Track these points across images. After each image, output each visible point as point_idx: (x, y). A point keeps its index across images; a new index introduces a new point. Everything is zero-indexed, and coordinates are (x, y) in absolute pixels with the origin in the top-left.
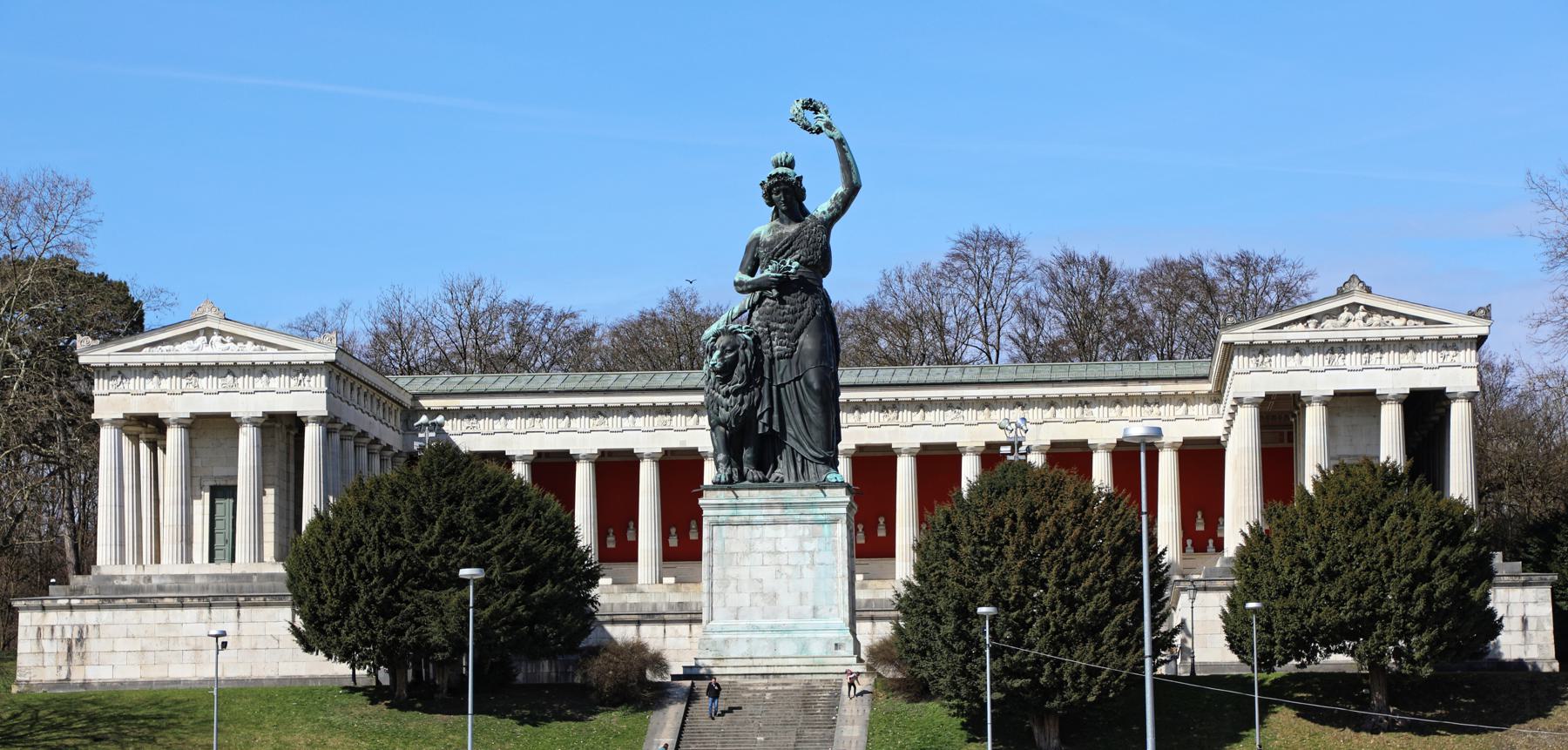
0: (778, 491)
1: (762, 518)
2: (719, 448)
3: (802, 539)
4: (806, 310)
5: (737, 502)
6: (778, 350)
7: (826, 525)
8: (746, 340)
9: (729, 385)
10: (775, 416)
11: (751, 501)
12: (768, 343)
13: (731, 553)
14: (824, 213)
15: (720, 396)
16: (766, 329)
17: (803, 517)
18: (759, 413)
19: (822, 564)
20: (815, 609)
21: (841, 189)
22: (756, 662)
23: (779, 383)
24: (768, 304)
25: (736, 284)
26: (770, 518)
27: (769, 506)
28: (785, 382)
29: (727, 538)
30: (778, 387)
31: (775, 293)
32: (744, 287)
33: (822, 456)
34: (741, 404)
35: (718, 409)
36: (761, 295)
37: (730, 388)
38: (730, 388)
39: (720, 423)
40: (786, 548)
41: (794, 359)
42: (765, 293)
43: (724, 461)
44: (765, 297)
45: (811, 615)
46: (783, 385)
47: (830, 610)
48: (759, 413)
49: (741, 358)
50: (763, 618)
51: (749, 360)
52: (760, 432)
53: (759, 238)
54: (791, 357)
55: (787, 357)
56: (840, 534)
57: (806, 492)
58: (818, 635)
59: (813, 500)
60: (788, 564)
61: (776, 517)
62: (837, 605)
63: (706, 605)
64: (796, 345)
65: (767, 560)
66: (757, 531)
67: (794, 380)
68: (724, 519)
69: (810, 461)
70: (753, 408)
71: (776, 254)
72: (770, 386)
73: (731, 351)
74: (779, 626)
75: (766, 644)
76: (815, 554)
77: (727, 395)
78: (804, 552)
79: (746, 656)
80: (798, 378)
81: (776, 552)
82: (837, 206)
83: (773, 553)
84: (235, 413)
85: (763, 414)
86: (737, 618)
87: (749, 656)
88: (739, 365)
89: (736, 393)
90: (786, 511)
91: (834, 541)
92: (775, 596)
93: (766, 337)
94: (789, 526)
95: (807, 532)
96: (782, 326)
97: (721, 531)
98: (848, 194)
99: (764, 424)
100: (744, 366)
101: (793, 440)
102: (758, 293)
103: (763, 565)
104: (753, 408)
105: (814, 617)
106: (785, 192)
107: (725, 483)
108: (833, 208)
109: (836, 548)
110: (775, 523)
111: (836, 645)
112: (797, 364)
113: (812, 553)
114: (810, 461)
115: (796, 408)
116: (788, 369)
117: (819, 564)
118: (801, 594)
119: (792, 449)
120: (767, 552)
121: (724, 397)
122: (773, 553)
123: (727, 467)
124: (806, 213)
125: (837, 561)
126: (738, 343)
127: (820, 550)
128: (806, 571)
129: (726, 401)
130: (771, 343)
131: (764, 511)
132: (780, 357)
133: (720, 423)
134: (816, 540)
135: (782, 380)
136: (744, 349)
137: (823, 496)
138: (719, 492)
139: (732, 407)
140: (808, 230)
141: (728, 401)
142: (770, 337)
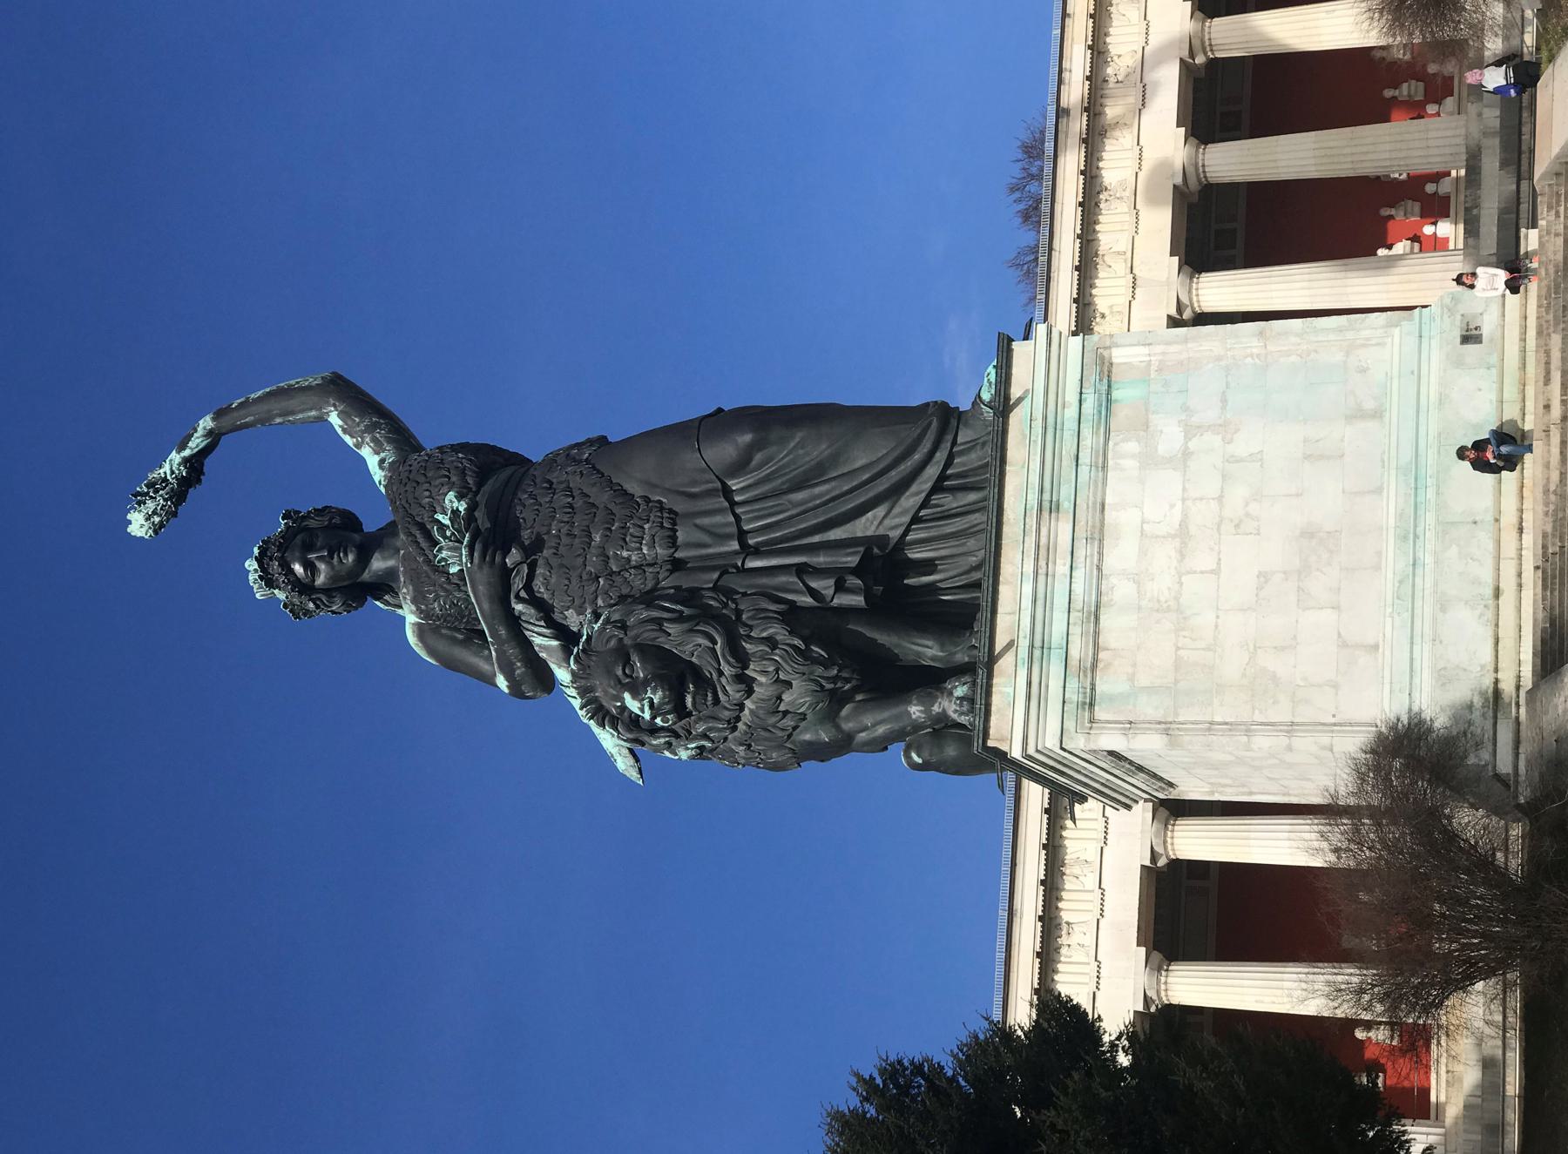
0: (1006, 529)
1: (1079, 574)
2: (897, 718)
3: (1149, 460)
4: (575, 482)
5: (1024, 644)
6: (652, 546)
7: (1115, 394)
8: (607, 621)
9: (721, 673)
10: (821, 560)
11: (1027, 603)
12: (631, 575)
13: (1178, 665)
14: (382, 461)
15: (748, 703)
16: (601, 581)
17: (1085, 458)
18: (807, 600)
19: (1224, 401)
20: (1357, 415)
21: (335, 419)
22: (1508, 585)
23: (735, 546)
24: (547, 585)
25: (516, 690)
26: (1080, 553)
27: (1043, 553)
28: (734, 530)
29: (1132, 678)
30: (748, 551)
31: (513, 557)
32: (512, 651)
33: (935, 424)
34: (772, 642)
35: (786, 713)
36: (520, 599)
37: (727, 670)
38: (727, 670)
39: (831, 716)
40: (1172, 506)
41: (680, 506)
42: (518, 583)
43: (928, 701)
44: (528, 587)
45: (1371, 425)
46: (742, 535)
47: (1363, 371)
48: (807, 600)
49: (648, 635)
50: (1377, 568)
51: (655, 614)
52: (858, 600)
53: (419, 624)
54: (671, 511)
55: (674, 524)
56: (1145, 350)
57: (1015, 451)
58: (1433, 396)
59: (1038, 424)
60: (1220, 499)
61: (1080, 533)
62: (1348, 354)
63: (1325, 739)
64: (647, 500)
65: (1205, 561)
66: (1120, 590)
67: (733, 504)
68: (1073, 684)
69: (949, 463)
70: (792, 616)
71: (424, 544)
72: (743, 571)
73: (627, 662)
74: (1400, 516)
75: (1453, 551)
77: (747, 684)
78: (1187, 454)
79: (1490, 614)
80: (727, 493)
81: (1183, 534)
82: (371, 429)
83: (1184, 543)
85: (813, 593)
86: (1376, 647)
87: (1491, 602)
88: (662, 641)
89: (742, 659)
90: (1067, 505)
91: (1159, 370)
92: (1312, 535)
93: (618, 579)
94: (1107, 501)
95: (1132, 446)
96: (597, 538)
97: (1111, 699)
98: (341, 399)
99: (840, 587)
100: (667, 626)
101: (896, 510)
102: (519, 607)
103: (1216, 572)
104: (792, 616)
105: (1381, 417)
106: (309, 547)
107: (974, 683)
108: (374, 440)
109: (1181, 363)
110: (1098, 536)
111: (1466, 339)
112: (693, 496)
113: (1190, 431)
114: (949, 463)
115: (799, 496)
116: (705, 521)
117: (1224, 408)
118: (1307, 457)
119: (916, 519)
120: (1182, 555)
121: (750, 692)
122: (1184, 543)
123: (942, 690)
124: (393, 524)
125: (1219, 358)
126: (613, 643)
127: (1186, 409)
128: (1240, 447)
129: (763, 686)
130: (635, 567)
131: (1062, 568)
132: (673, 542)
133: (831, 716)
134: (1157, 421)
135: (728, 537)
136: (624, 627)
137: (1026, 403)
138: (997, 700)
139: (777, 671)
140: (402, 490)
141: (762, 679)
142: (619, 572)
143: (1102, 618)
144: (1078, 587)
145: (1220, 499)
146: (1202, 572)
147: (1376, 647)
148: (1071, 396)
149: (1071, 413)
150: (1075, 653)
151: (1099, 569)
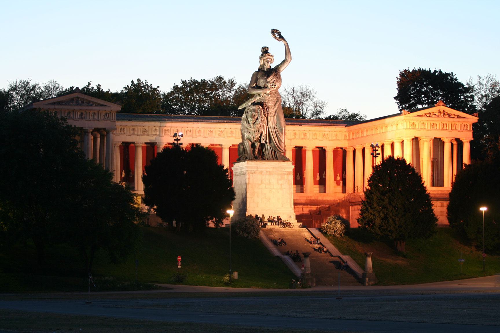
1: (265, 172)
13: (256, 184)
26: (268, 172)
60: (274, 188)
76: (283, 185)
78: (279, 184)
84: (85, 127)
103: (266, 188)
113: (281, 185)
120: (268, 184)
143: (260, 175)
144: (264, 172)
145: (274, 188)
146: (266, 187)
147: (257, 206)
148: (285, 170)
149: (284, 170)
150: (257, 172)
151: (266, 174)
